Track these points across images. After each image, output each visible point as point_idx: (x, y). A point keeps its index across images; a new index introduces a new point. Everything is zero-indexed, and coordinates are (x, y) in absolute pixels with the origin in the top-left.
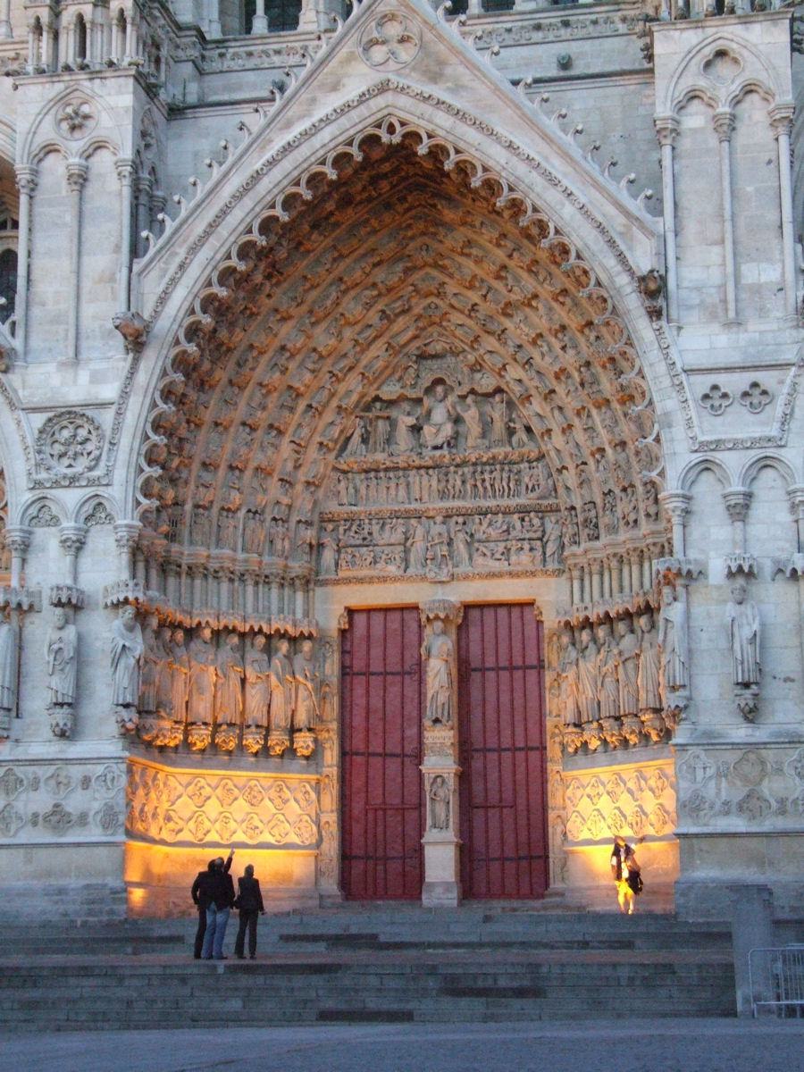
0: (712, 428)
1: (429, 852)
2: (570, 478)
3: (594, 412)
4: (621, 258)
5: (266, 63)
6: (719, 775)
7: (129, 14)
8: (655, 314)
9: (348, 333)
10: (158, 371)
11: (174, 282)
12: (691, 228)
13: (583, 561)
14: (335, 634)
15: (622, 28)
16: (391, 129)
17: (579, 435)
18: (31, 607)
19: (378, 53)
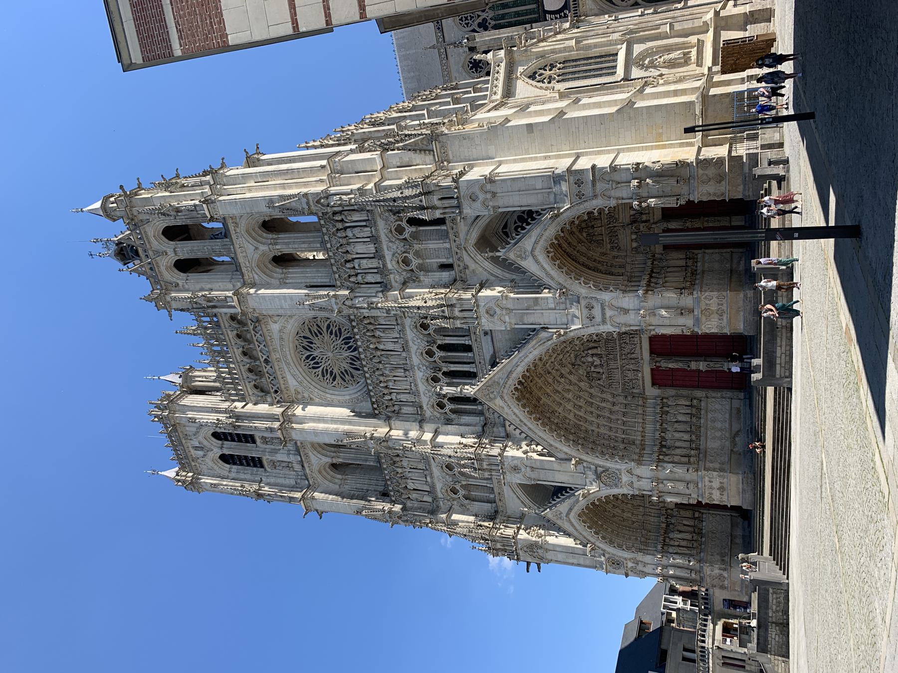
0: (598, 318)
9: (567, 387)
12: (537, 321)
14: (660, 390)
16: (514, 394)
18: (658, 490)
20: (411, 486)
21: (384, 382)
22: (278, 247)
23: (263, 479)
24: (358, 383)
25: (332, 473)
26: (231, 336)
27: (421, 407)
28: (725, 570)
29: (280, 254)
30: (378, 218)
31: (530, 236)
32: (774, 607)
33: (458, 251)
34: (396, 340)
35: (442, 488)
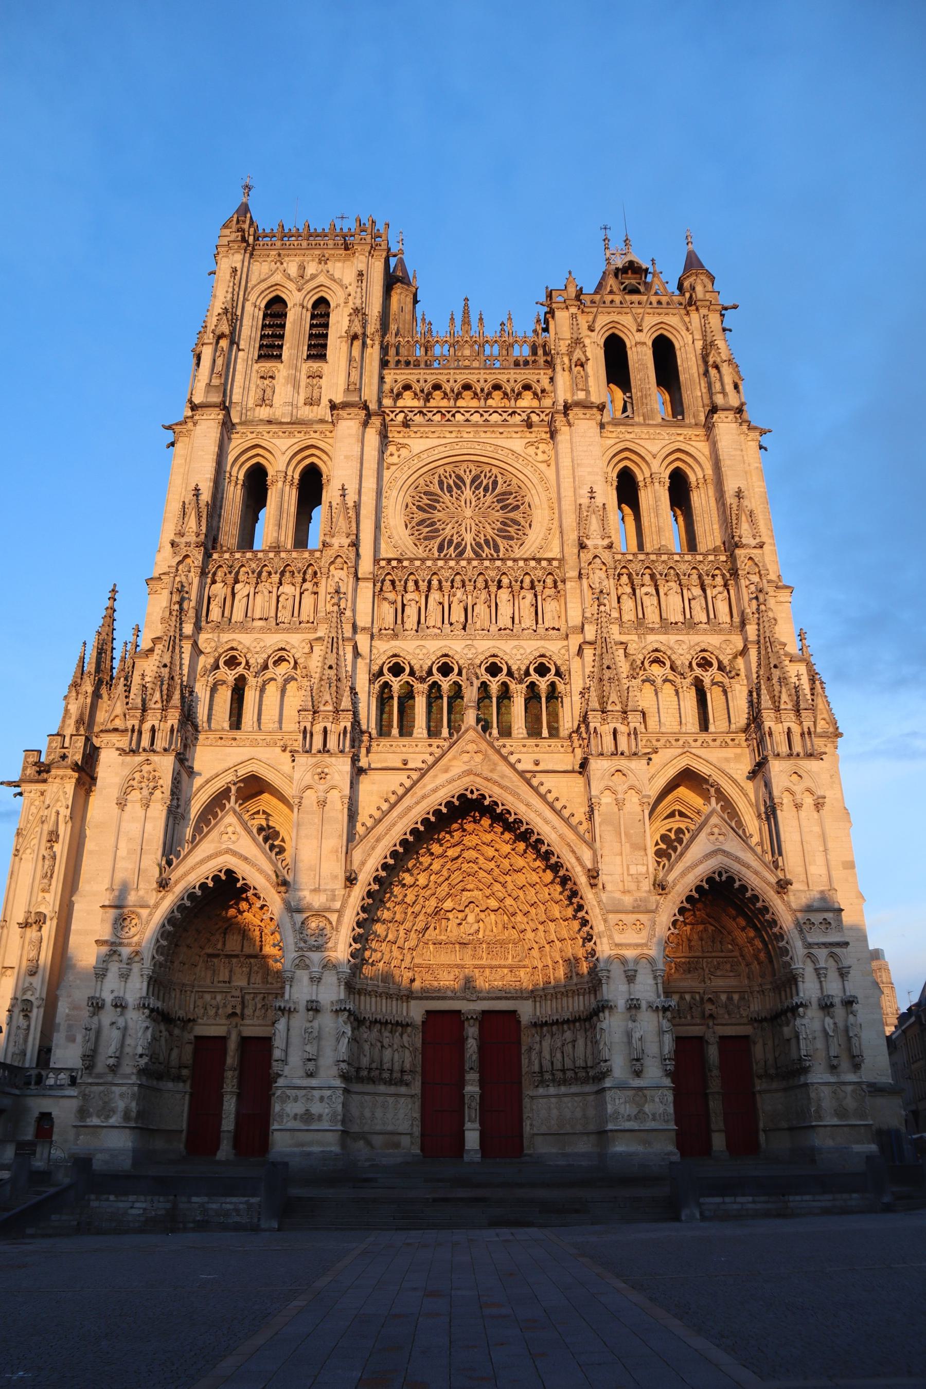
0: (618, 938)
1: (467, 1134)
2: (535, 953)
3: (550, 923)
4: (578, 859)
5: (398, 750)
6: (626, 1102)
7: (349, 729)
8: (593, 886)
10: (360, 897)
11: (369, 855)
13: (541, 993)
14: (420, 1023)
15: (562, 750)
16: (472, 792)
17: (541, 933)
19: (466, 757)
20: (242, 589)
21: (440, 588)
22: (657, 484)
23: (241, 354)
24: (416, 545)
25: (248, 465)
26: (499, 376)
27: (395, 636)
28: (126, 1116)
29: (641, 484)
30: (723, 638)
31: (744, 851)
32: (214, 1206)
33: (681, 742)
34: (516, 621)
35: (240, 643)
